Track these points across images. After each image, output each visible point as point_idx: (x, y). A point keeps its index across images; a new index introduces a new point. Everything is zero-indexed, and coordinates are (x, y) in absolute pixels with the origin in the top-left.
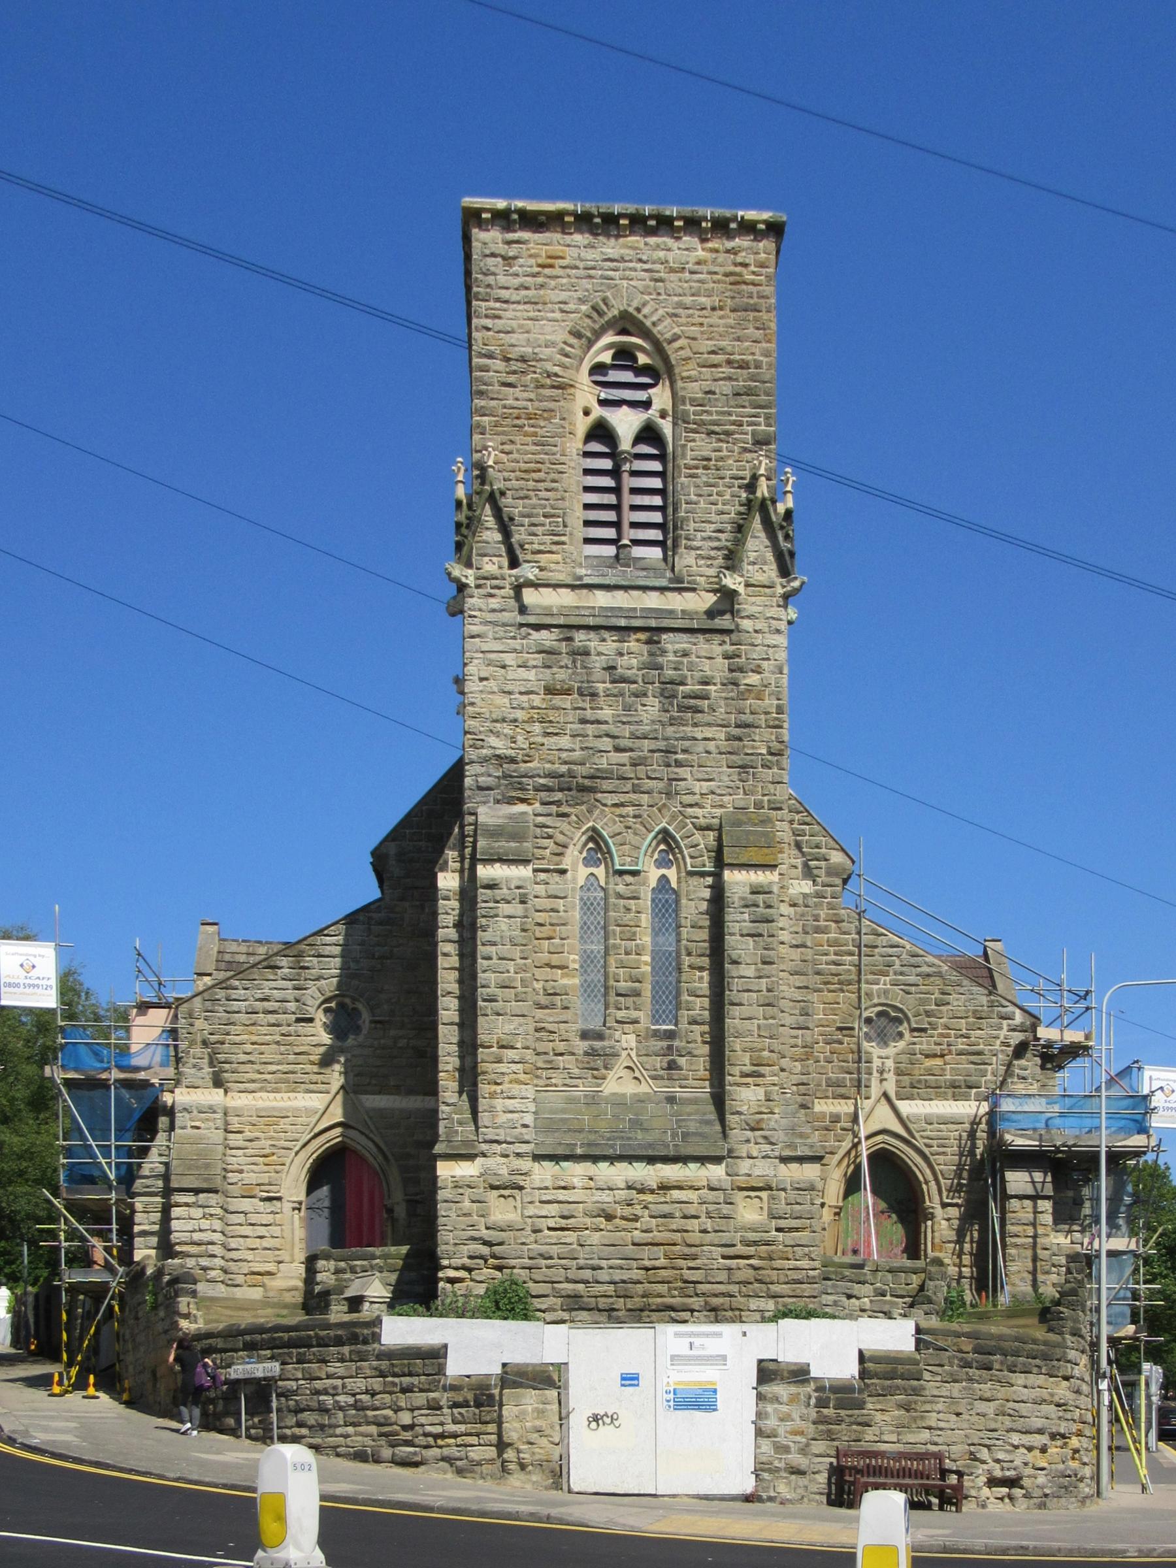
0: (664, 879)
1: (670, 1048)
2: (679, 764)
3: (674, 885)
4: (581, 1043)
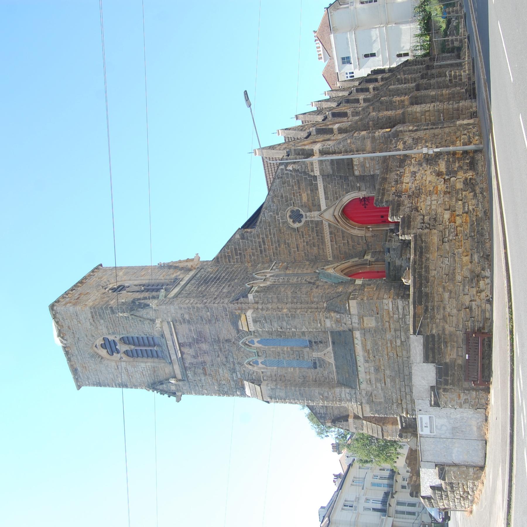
0: (258, 342)
1: (315, 342)
2: (219, 338)
3: (259, 339)
4: (318, 368)
